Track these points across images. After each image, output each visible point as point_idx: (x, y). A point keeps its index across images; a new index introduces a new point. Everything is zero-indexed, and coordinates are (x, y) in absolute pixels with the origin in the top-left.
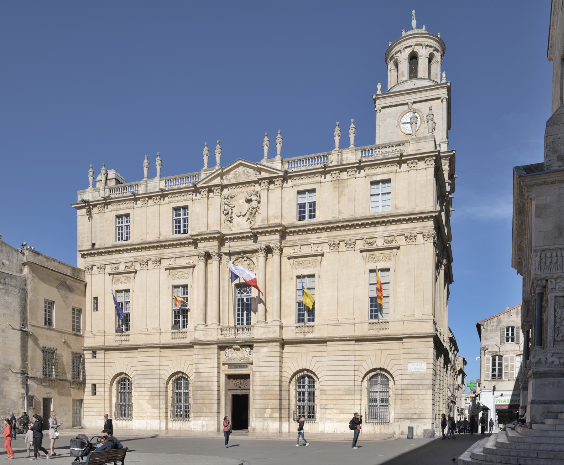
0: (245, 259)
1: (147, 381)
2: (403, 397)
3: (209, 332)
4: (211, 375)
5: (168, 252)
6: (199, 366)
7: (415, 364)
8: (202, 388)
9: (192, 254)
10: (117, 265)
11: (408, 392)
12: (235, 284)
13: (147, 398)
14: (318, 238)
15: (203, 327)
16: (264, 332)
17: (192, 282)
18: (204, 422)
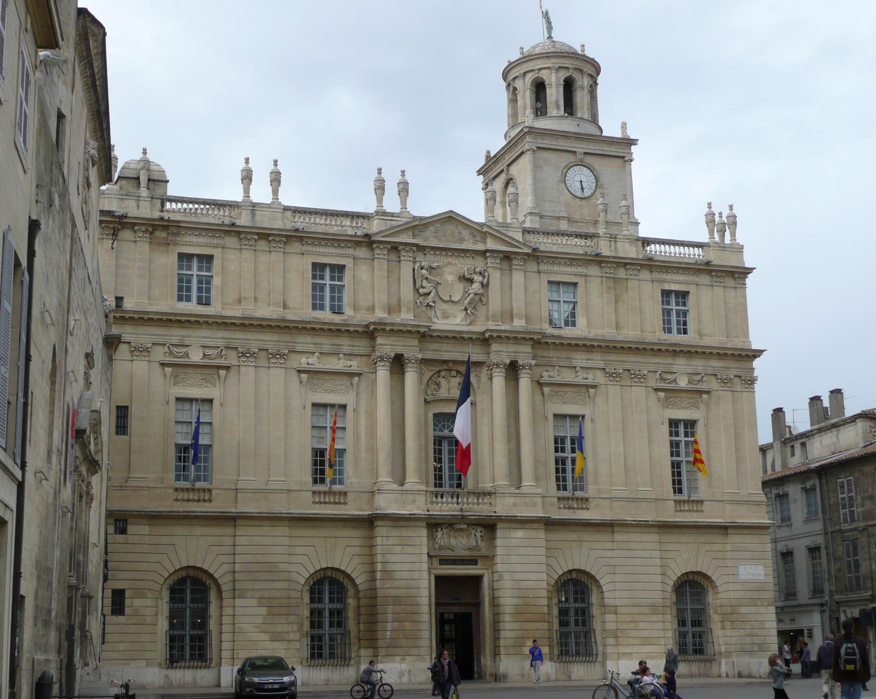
0: (454, 373)
1: (258, 585)
2: (734, 617)
3: (410, 497)
4: (416, 575)
5: (304, 342)
6: (390, 558)
7: (749, 567)
8: (397, 600)
9: (356, 352)
10: (184, 350)
11: (743, 610)
12: (435, 415)
13: (260, 620)
14: (588, 360)
15: (395, 486)
16: (515, 505)
17: (357, 402)
18: (404, 666)
